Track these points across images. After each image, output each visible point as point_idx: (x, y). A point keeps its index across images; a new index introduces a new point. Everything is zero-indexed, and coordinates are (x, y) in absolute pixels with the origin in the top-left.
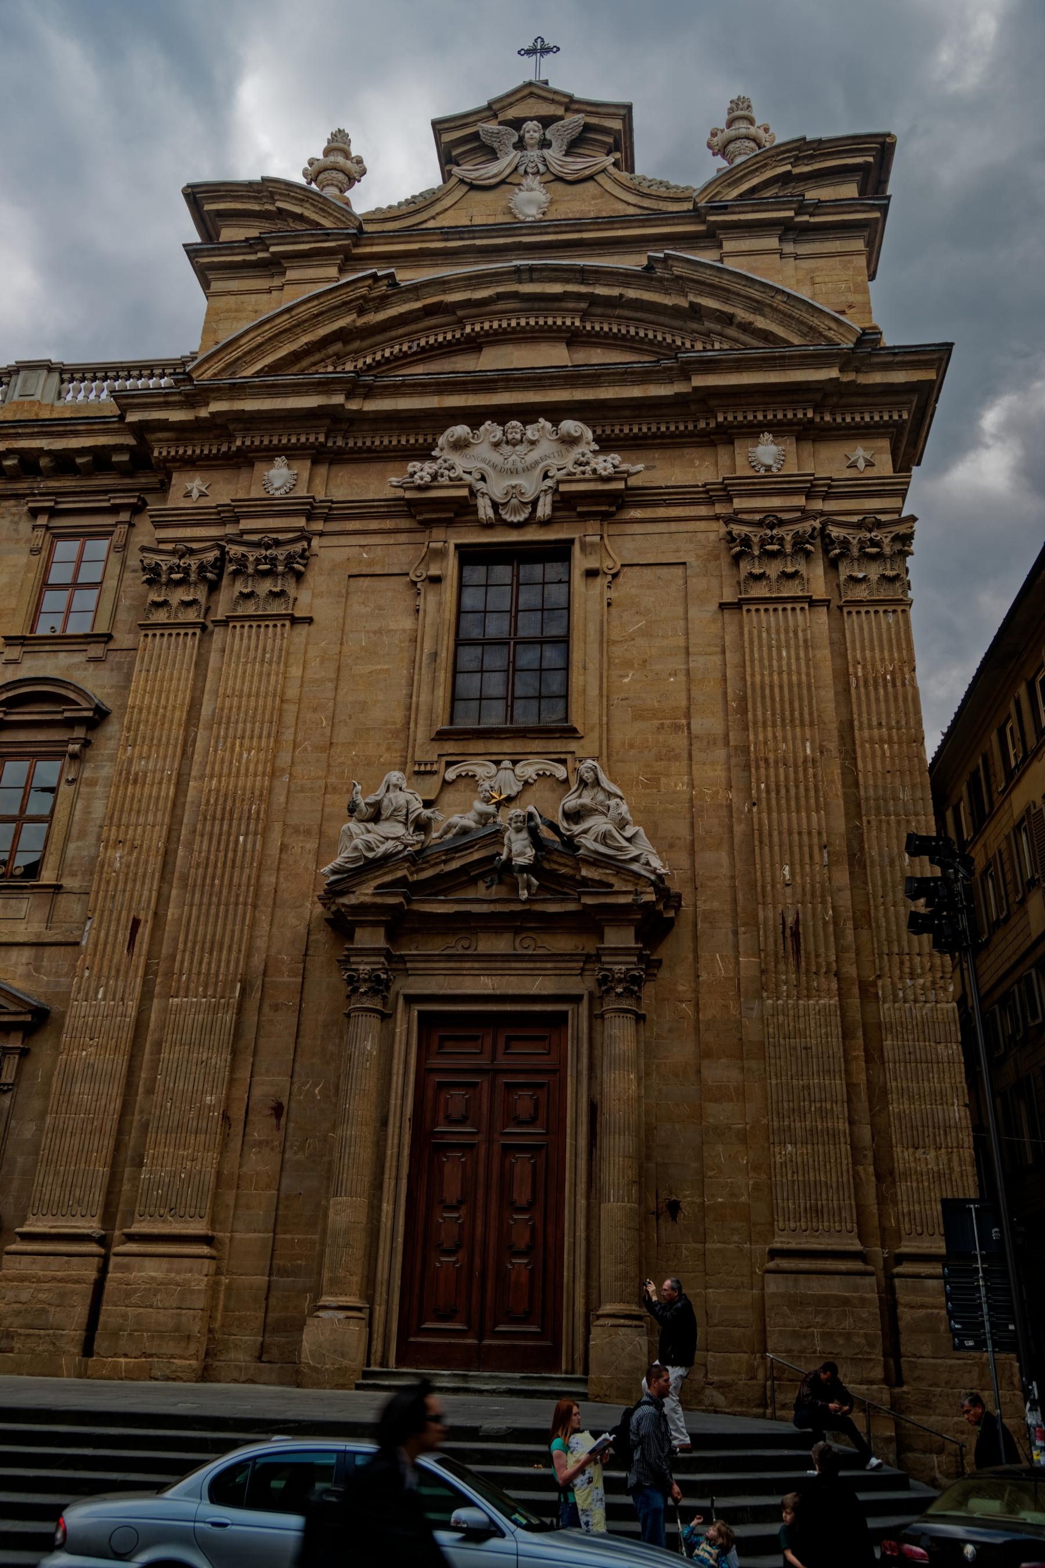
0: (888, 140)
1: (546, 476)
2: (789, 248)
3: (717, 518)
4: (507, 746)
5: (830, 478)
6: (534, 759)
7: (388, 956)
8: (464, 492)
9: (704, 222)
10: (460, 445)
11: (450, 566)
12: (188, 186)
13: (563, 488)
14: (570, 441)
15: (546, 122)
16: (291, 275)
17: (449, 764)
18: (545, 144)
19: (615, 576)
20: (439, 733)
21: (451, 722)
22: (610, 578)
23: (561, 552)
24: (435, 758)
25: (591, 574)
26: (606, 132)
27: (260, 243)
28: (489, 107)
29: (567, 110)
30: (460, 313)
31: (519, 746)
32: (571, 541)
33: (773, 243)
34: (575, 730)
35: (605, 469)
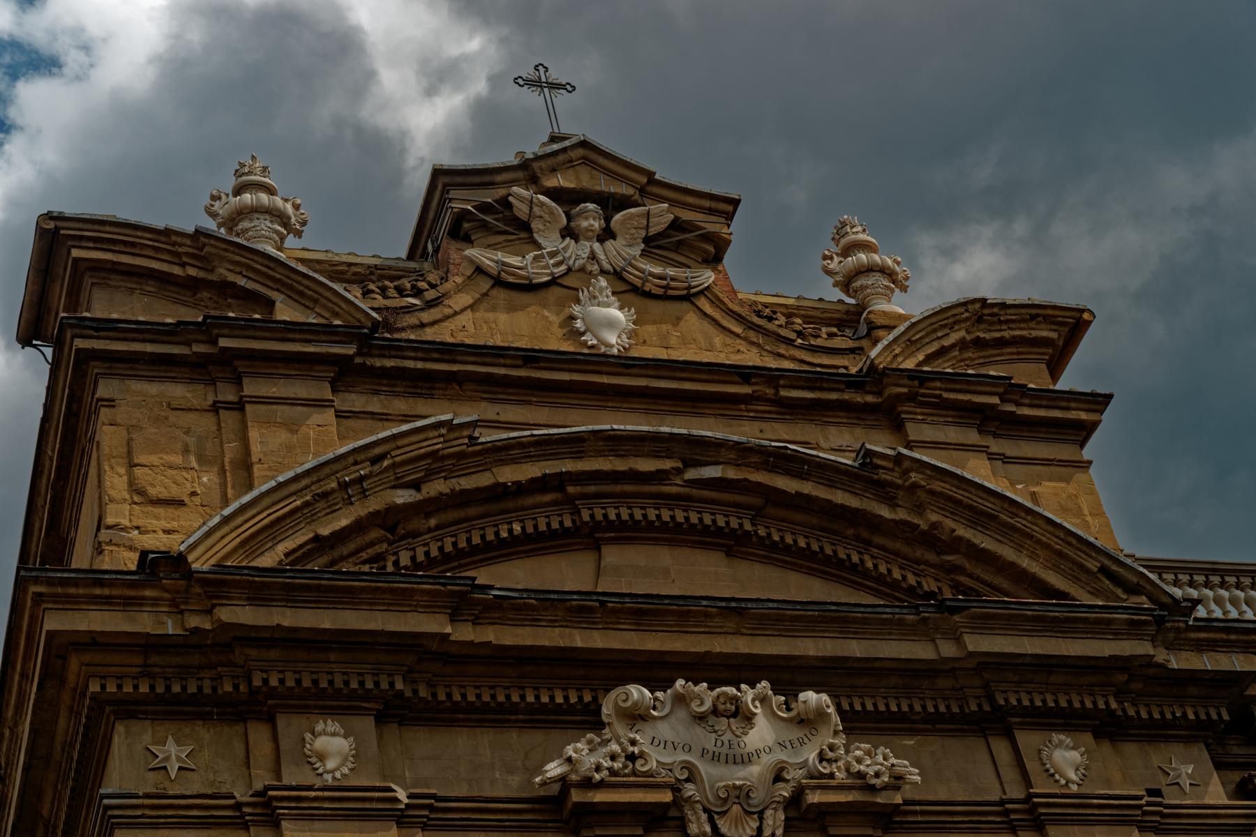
0: (1086, 316)
1: (778, 778)
2: (996, 446)
8: (667, 797)
9: (879, 394)
10: (636, 717)
12: (49, 216)
13: (814, 798)
14: (809, 722)
15: (609, 204)
16: (251, 388)
18: (607, 234)
26: (695, 231)
27: (208, 330)
28: (525, 165)
29: (642, 191)
30: (571, 489)
33: (972, 437)
35: (877, 775)
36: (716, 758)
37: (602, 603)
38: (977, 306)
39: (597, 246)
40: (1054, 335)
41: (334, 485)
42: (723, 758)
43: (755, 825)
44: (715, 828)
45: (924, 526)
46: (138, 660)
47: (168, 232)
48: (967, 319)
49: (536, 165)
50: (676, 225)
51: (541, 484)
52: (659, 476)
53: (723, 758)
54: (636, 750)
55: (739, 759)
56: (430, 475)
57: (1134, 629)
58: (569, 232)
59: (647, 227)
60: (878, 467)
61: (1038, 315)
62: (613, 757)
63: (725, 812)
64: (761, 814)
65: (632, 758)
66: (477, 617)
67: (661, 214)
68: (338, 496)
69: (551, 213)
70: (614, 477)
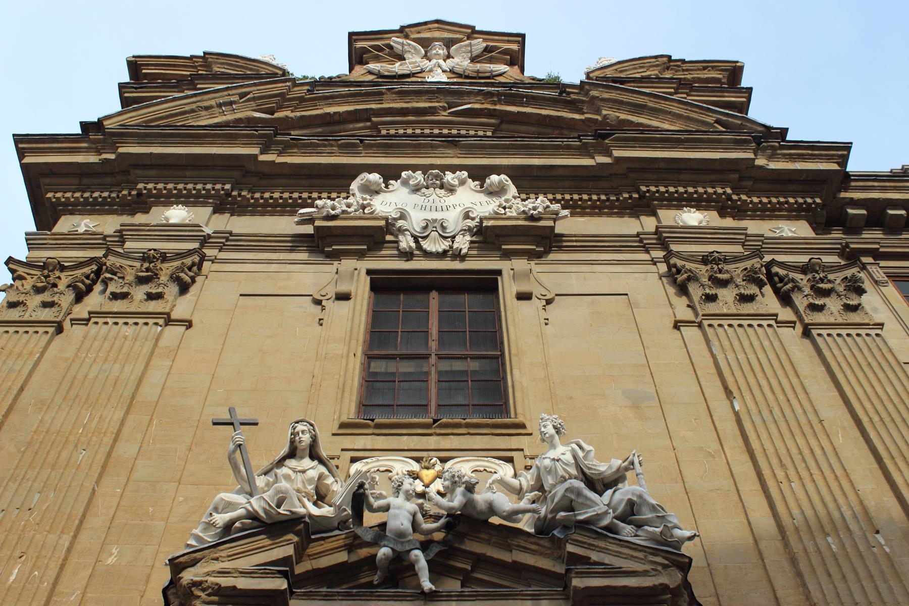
3: (654, 262)
4: (432, 442)
5: (762, 236)
6: (469, 456)
8: (382, 223)
11: (361, 288)
17: (354, 460)
19: (549, 302)
20: (343, 426)
22: (544, 303)
23: (487, 284)
25: (524, 297)
32: (499, 272)
34: (523, 426)
36: (423, 208)
37: (361, 141)
38: (665, 59)
39: (441, 62)
40: (721, 76)
41: (213, 103)
42: (428, 208)
43: (447, 244)
44: (419, 247)
45: (600, 118)
46: (76, 181)
47: (192, 57)
48: (657, 66)
49: (407, 30)
50: (487, 50)
51: (355, 117)
52: (432, 111)
53: (428, 208)
54: (365, 202)
55: (439, 208)
56: (280, 107)
57: (738, 144)
58: (426, 57)
59: (471, 52)
60: (569, 93)
61: (708, 67)
62: (349, 206)
63: (428, 236)
64: (454, 237)
65: (364, 207)
66: (281, 153)
67: (479, 44)
68: (217, 110)
69: (415, 49)
70: (403, 112)
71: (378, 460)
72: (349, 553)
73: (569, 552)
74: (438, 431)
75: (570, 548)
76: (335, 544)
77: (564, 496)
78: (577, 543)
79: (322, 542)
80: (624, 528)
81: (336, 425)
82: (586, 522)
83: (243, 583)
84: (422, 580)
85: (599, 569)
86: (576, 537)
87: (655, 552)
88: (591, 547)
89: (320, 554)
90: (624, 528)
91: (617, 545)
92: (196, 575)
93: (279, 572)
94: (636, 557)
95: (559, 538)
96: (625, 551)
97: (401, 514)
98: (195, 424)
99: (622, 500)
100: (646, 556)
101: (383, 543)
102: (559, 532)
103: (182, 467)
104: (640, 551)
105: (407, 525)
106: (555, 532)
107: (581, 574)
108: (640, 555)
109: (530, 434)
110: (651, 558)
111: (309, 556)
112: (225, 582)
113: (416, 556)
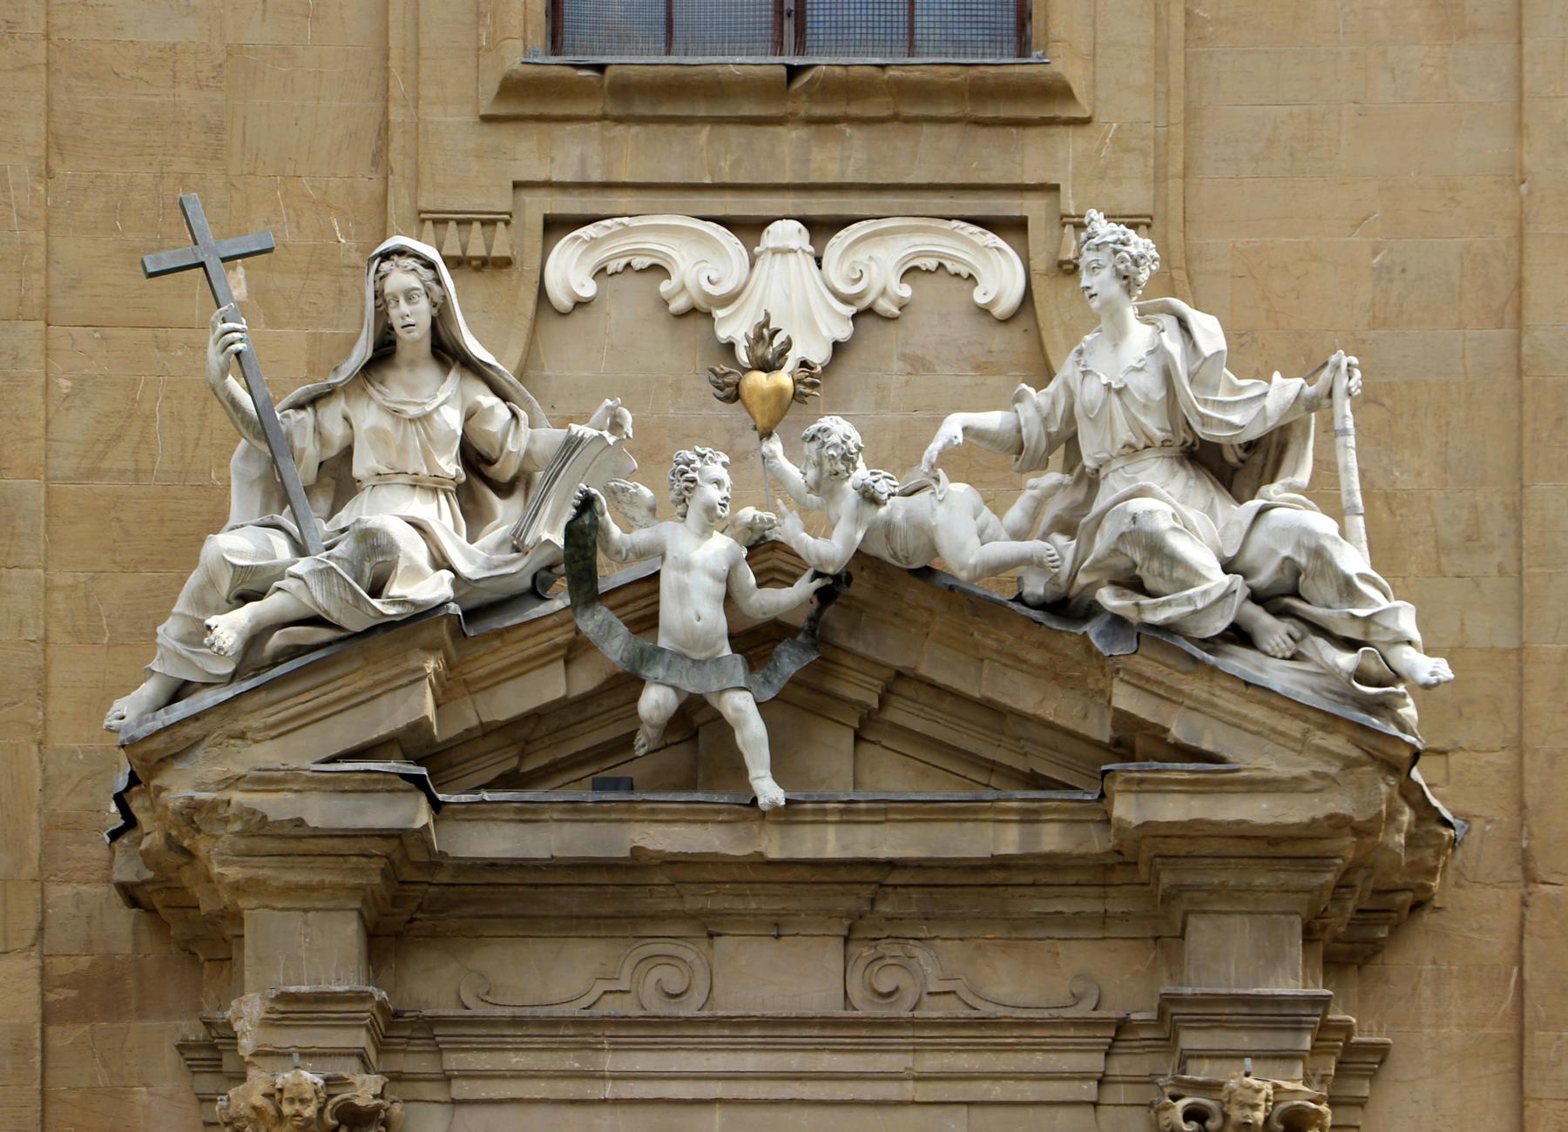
4: (789, 152)
7: (396, 1028)
17: (556, 226)
21: (555, 42)
24: (501, 202)
31: (845, 156)
71: (627, 230)
72: (567, 662)
73: (1117, 710)
74: (804, 108)
75: (1125, 699)
76: (530, 647)
77: (1114, 551)
78: (1142, 684)
79: (497, 643)
80: (1269, 631)
81: (493, 87)
82: (1168, 629)
83: (320, 811)
84: (753, 774)
85: (1181, 770)
86: (1145, 666)
87: (1330, 721)
88: (1170, 696)
89: (498, 678)
90: (1269, 631)
91: (1242, 695)
92: (201, 786)
93: (405, 777)
94: (1281, 734)
95: (1099, 654)
96: (1257, 713)
97: (697, 571)
98: (40, 57)
99: (1272, 552)
100: (1306, 733)
101: (650, 674)
102: (1101, 635)
103: (39, 255)
104: (1295, 716)
105: (713, 619)
106: (1092, 630)
107: (1141, 786)
108: (1293, 727)
109: (1086, 121)
110: (1319, 738)
111: (466, 683)
112: (277, 805)
113: (738, 710)
